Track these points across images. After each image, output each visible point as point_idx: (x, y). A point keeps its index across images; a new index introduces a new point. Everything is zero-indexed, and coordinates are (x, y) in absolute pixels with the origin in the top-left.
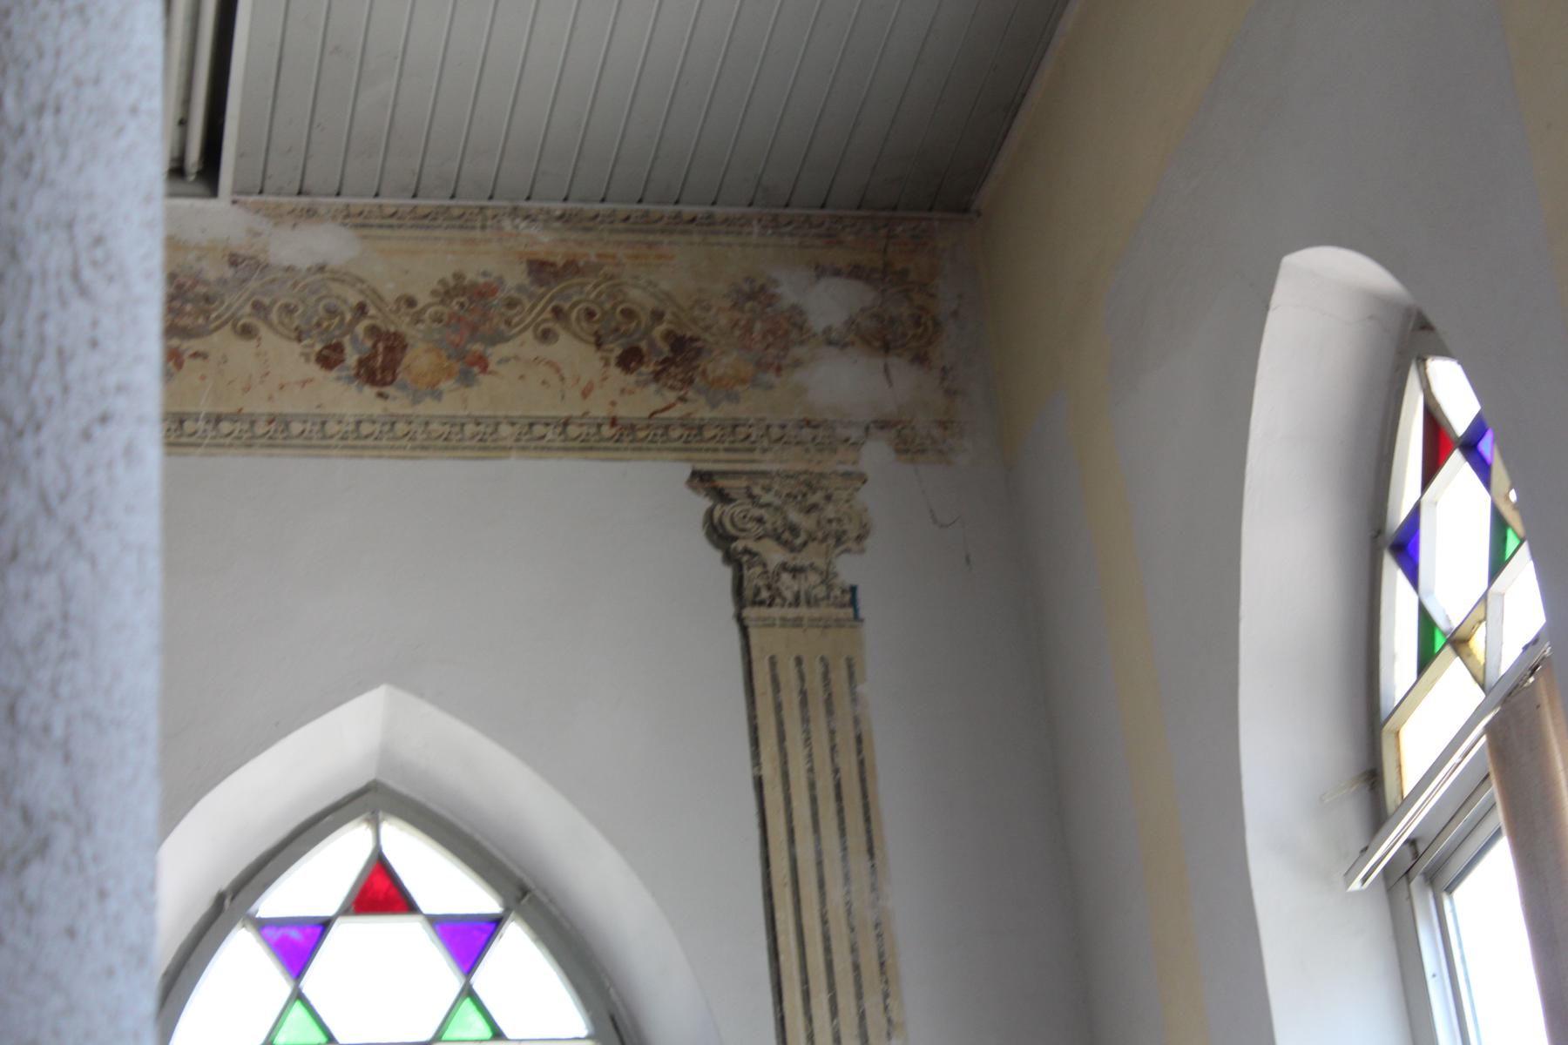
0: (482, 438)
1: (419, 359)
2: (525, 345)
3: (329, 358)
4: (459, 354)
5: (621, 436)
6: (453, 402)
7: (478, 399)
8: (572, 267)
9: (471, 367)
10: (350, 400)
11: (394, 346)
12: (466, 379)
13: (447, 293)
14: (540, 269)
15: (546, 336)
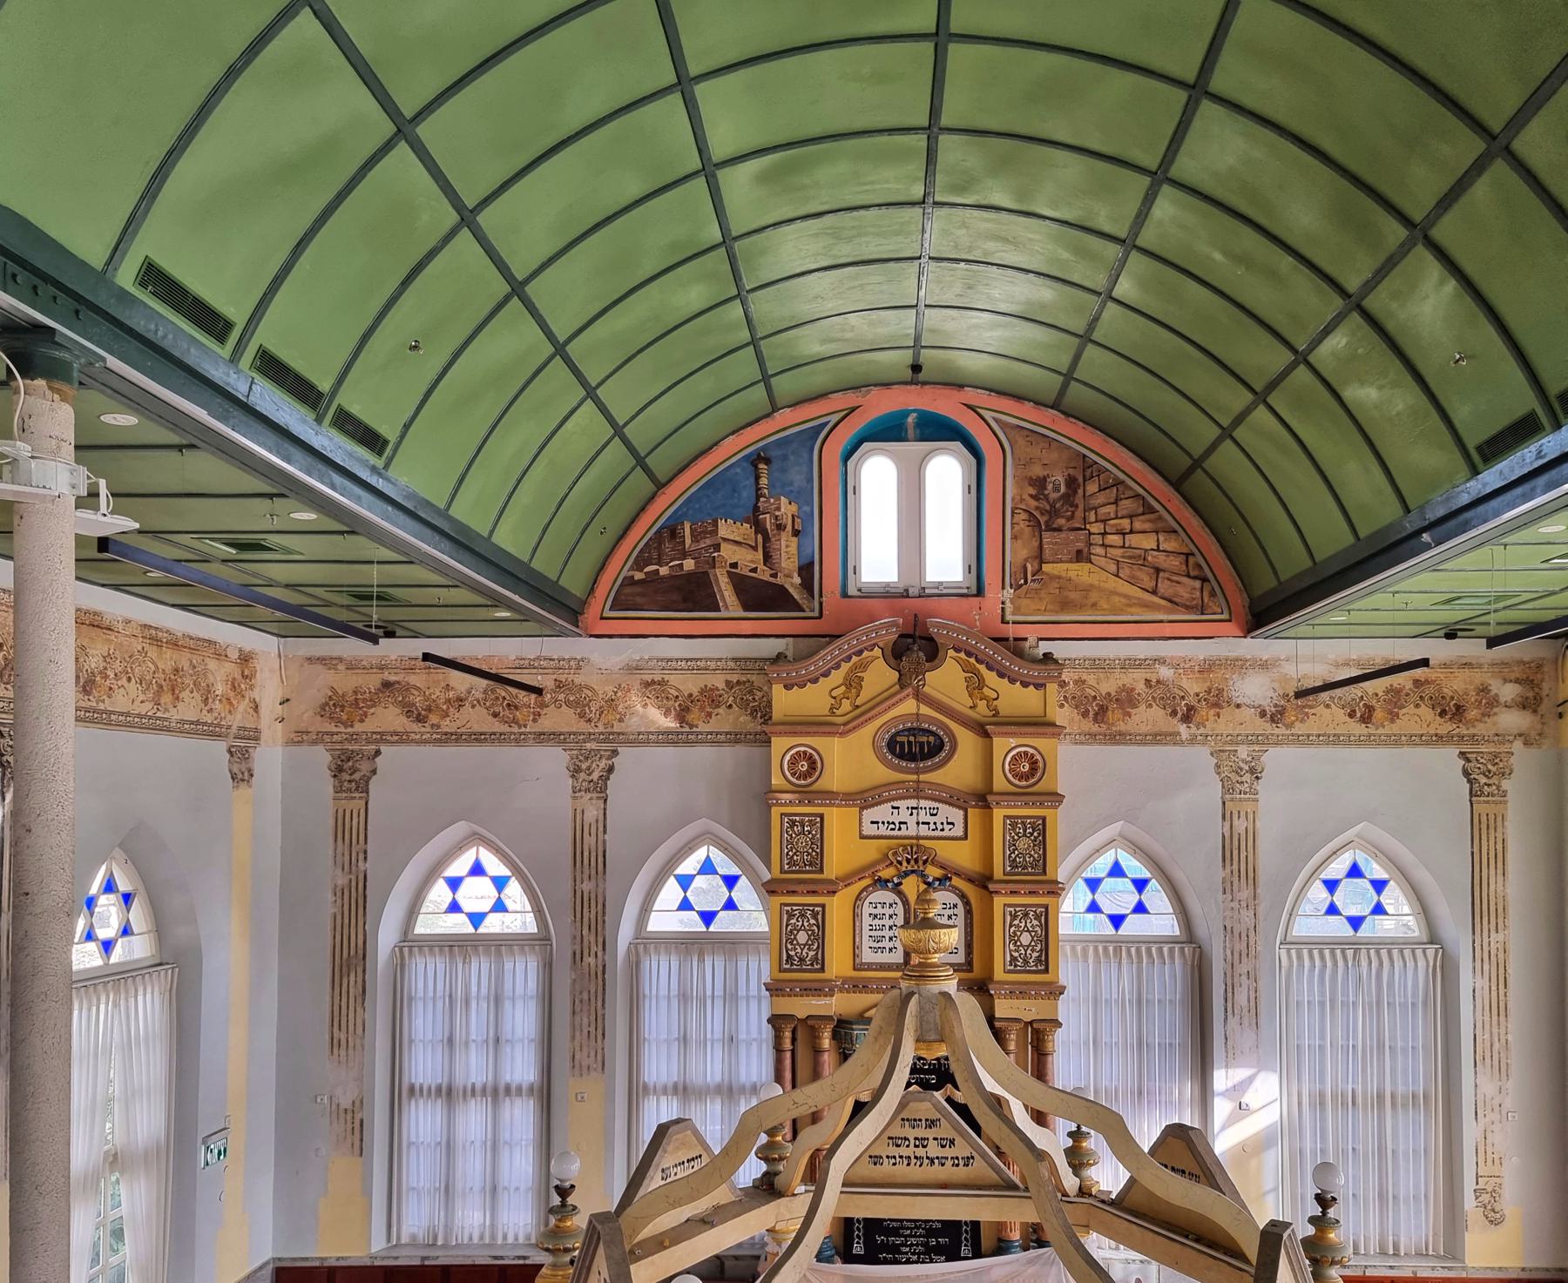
0: (1395, 741)
1: (1379, 714)
2: (1410, 709)
3: (1352, 715)
4: (1391, 713)
5: (1439, 740)
6: (1390, 729)
7: (1393, 729)
8: (1427, 682)
9: (1393, 717)
10: (1358, 729)
11: (1370, 709)
12: (1392, 721)
13: (1387, 692)
15: (1417, 706)
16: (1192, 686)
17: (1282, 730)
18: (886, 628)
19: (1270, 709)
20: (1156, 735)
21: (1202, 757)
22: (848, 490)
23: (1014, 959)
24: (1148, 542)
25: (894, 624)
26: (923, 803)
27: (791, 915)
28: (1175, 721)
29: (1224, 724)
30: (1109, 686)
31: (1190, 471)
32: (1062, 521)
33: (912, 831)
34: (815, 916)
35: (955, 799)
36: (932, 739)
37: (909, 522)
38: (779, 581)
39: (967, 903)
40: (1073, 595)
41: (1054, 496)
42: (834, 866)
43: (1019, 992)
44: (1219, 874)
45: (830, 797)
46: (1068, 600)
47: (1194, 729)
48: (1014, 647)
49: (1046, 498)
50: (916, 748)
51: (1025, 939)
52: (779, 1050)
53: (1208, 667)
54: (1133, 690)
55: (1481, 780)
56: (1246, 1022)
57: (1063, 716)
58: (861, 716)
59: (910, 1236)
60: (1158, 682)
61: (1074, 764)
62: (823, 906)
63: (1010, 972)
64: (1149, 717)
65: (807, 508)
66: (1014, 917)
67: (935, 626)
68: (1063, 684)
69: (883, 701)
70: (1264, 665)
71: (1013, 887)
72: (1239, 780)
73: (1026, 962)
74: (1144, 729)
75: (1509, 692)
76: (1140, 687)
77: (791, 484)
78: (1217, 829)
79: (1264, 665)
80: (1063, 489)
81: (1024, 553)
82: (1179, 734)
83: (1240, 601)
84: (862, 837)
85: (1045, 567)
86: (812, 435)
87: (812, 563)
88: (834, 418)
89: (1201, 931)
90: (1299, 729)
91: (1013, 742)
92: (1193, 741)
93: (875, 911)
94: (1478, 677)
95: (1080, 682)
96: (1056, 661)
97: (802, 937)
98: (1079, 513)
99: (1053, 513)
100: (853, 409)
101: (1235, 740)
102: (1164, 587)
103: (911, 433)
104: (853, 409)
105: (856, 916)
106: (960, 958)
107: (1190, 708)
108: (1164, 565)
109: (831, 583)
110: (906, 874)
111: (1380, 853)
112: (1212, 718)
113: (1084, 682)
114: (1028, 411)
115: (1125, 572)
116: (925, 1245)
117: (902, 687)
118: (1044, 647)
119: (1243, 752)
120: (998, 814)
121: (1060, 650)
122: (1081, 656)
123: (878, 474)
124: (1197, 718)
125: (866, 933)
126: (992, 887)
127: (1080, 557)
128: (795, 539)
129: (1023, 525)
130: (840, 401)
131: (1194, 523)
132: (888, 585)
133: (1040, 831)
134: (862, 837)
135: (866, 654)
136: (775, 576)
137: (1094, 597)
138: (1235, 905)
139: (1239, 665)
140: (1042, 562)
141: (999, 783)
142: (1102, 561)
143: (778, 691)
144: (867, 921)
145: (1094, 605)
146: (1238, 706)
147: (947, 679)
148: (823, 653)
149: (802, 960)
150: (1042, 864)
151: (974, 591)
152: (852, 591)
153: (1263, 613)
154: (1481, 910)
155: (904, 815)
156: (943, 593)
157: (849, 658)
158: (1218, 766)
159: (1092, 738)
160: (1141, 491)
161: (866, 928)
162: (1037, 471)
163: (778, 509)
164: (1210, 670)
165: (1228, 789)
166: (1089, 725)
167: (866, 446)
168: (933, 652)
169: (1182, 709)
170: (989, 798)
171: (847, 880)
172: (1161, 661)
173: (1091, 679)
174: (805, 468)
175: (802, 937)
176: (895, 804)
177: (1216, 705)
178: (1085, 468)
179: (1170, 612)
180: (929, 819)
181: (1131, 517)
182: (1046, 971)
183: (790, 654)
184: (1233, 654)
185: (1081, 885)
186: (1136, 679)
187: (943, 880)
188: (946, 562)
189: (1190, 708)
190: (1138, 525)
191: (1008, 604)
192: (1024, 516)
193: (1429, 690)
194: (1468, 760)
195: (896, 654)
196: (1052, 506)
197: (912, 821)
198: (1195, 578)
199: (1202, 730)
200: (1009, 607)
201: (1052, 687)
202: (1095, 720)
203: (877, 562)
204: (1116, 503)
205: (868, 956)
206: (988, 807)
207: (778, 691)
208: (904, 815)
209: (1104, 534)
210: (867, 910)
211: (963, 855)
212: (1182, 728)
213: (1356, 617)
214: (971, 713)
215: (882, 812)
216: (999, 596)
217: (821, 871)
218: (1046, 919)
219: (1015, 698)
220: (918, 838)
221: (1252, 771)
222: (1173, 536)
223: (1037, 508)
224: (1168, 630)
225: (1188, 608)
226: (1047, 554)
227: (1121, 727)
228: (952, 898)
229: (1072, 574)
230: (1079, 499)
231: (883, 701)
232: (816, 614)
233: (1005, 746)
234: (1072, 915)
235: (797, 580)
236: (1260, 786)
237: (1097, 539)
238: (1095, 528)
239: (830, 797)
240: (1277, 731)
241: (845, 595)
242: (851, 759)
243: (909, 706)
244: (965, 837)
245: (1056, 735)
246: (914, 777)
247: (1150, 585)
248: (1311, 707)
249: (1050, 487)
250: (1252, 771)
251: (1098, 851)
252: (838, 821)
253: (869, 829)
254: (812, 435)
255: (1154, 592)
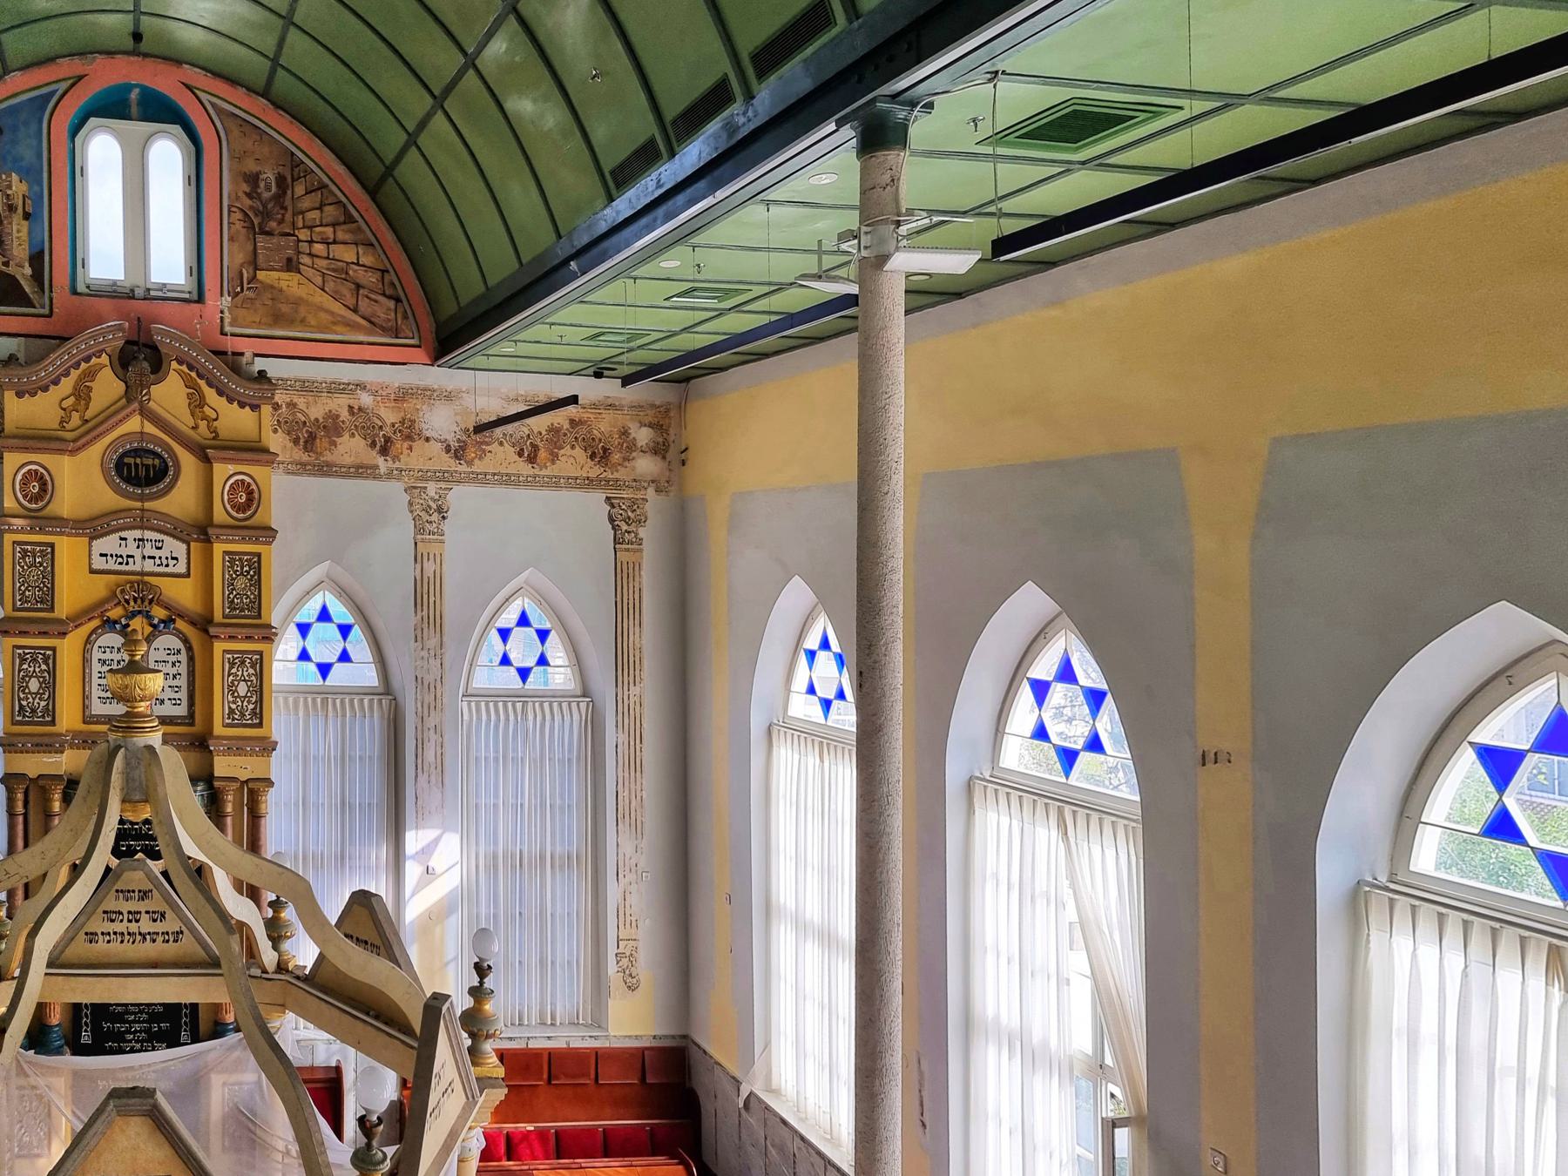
0: (555, 483)
1: (542, 454)
2: (567, 450)
3: (520, 454)
4: (552, 453)
5: (589, 483)
8: (581, 422)
9: (554, 458)
10: (525, 469)
11: (535, 447)
12: (553, 462)
14: (572, 421)
15: (573, 447)
16: (390, 416)
17: (464, 468)
18: (112, 333)
19: (454, 445)
20: (358, 467)
21: (395, 489)
22: (75, 172)
23: (232, 711)
24: (348, 254)
25: (120, 328)
26: (149, 534)
27: (23, 660)
28: (374, 453)
29: (419, 457)
30: (317, 412)
31: (383, 179)
32: (273, 224)
33: (137, 568)
34: (46, 662)
35: (178, 530)
36: (157, 462)
37: (133, 211)
38: (11, 270)
39: (189, 649)
40: (285, 308)
41: (266, 195)
42: (65, 605)
43: (238, 747)
44: (413, 620)
45: (60, 524)
46: (282, 313)
47: (390, 463)
48: (232, 361)
49: (259, 195)
50: (141, 471)
51: (242, 689)
52: (11, 814)
53: (403, 395)
54: (338, 416)
55: (623, 525)
56: (433, 778)
57: (276, 442)
58: (91, 431)
59: (134, 1021)
60: (360, 409)
61: (286, 494)
62: (54, 649)
63: (229, 726)
64: (351, 448)
65: (36, 188)
66: (232, 665)
67: (161, 334)
68: (276, 407)
69: (111, 416)
70: (449, 397)
71: (231, 631)
72: (430, 517)
73: (242, 715)
74: (348, 460)
75: (643, 436)
76: (344, 415)
77: (22, 159)
78: (409, 572)
79: (449, 397)
80: (274, 189)
81: (240, 258)
82: (377, 467)
83: (428, 325)
84: (92, 572)
85: (261, 275)
86: (41, 104)
87: (42, 252)
88: (64, 86)
89: (396, 682)
90: (479, 466)
91: (231, 468)
92: (389, 476)
93: (104, 657)
94: (621, 419)
95: (292, 405)
96: (269, 380)
97: (34, 685)
98: (288, 217)
99: (266, 215)
100: (80, 78)
101: (425, 476)
102: (364, 304)
103: (134, 110)
104: (80, 78)
105: (86, 661)
106: (181, 711)
107: (388, 440)
108: (363, 282)
109: (61, 279)
110: (133, 615)
111: (543, 600)
112: (406, 452)
113: (295, 405)
114: (239, 96)
115: (330, 286)
116: (148, 1031)
117: (129, 401)
118: (260, 364)
119: (432, 488)
120: (219, 549)
121: (274, 368)
122: (292, 376)
123: (102, 150)
124: (393, 451)
125: (95, 681)
126: (213, 631)
127: (291, 265)
128: (26, 223)
129: (239, 225)
130: (67, 68)
131: (388, 237)
132: (115, 283)
133: (254, 568)
134: (92, 572)
135: (94, 360)
136: (6, 264)
137: (303, 311)
138: (424, 654)
139: (427, 394)
140: (256, 269)
141: (219, 515)
142: (309, 272)
143: (9, 396)
144: (96, 667)
145: (303, 321)
146: (427, 439)
147: (170, 394)
148: (53, 356)
149: (33, 711)
150: (257, 606)
151: (195, 297)
152: (81, 288)
153: (448, 340)
154: (623, 663)
155: (131, 548)
156: (163, 296)
157: (77, 365)
158: (410, 504)
159: (302, 468)
160: (343, 199)
161: (95, 675)
162: (251, 166)
163: (10, 187)
164: (404, 400)
165: (419, 530)
166: (300, 455)
167: (93, 121)
168: (158, 365)
169: (380, 441)
170: (211, 531)
171: (77, 619)
172: (361, 386)
173: (301, 402)
174: (35, 143)
175: (34, 685)
176: (123, 534)
177: (409, 438)
178: (293, 170)
179: (370, 333)
180: (157, 553)
181: (333, 225)
182: (260, 725)
183: (22, 357)
184: (422, 383)
185: (292, 631)
186: (339, 404)
187: (168, 622)
188: (169, 264)
189: (388, 440)
190: (341, 236)
191: (227, 314)
192: (239, 215)
193: (583, 430)
194: (613, 506)
195: (123, 362)
196: (264, 206)
197: (138, 558)
198: (390, 297)
199: (397, 465)
200: (227, 321)
201: (266, 410)
202: (305, 448)
203: (105, 261)
204: (320, 208)
205: (98, 708)
206: (208, 541)
207: (9, 396)
208: (131, 548)
209: (311, 242)
210: (97, 655)
211: (183, 593)
212: (380, 461)
213: (523, 349)
214: (192, 433)
215: (109, 544)
216: (219, 303)
217: (52, 609)
218: (260, 665)
219: (234, 420)
220: (142, 574)
221: (440, 510)
222: (370, 249)
223: (251, 208)
224: (368, 353)
225: (385, 331)
226: (261, 259)
227: (328, 457)
228: (176, 643)
229: (283, 284)
230: (288, 202)
231: (111, 416)
232: (46, 311)
233: (223, 471)
234: (285, 666)
235: (28, 271)
236: (446, 526)
237: (304, 247)
238: (303, 235)
239: (60, 524)
240: (460, 468)
241: (75, 292)
242: (81, 482)
243: (134, 424)
244: (187, 575)
245: (270, 463)
246: (139, 504)
247: (351, 302)
248: (488, 444)
249: (262, 185)
250: (440, 510)
251: (308, 594)
252: (68, 549)
253: (99, 563)
254: (41, 104)
255: (355, 310)
